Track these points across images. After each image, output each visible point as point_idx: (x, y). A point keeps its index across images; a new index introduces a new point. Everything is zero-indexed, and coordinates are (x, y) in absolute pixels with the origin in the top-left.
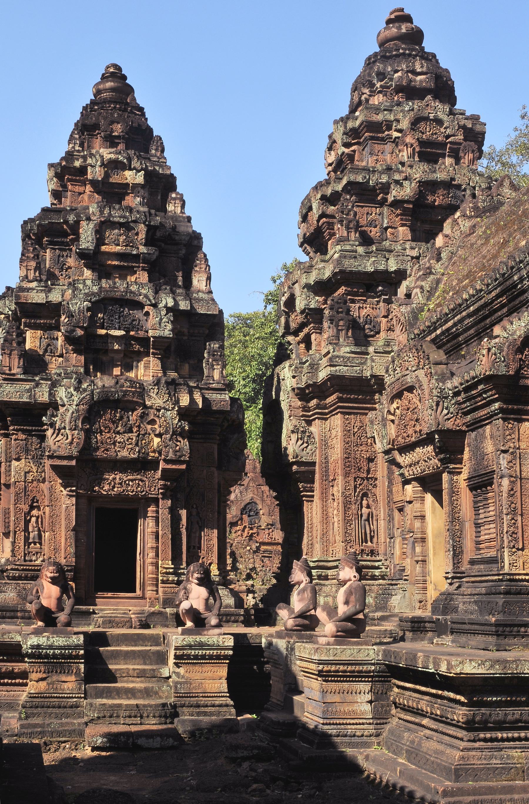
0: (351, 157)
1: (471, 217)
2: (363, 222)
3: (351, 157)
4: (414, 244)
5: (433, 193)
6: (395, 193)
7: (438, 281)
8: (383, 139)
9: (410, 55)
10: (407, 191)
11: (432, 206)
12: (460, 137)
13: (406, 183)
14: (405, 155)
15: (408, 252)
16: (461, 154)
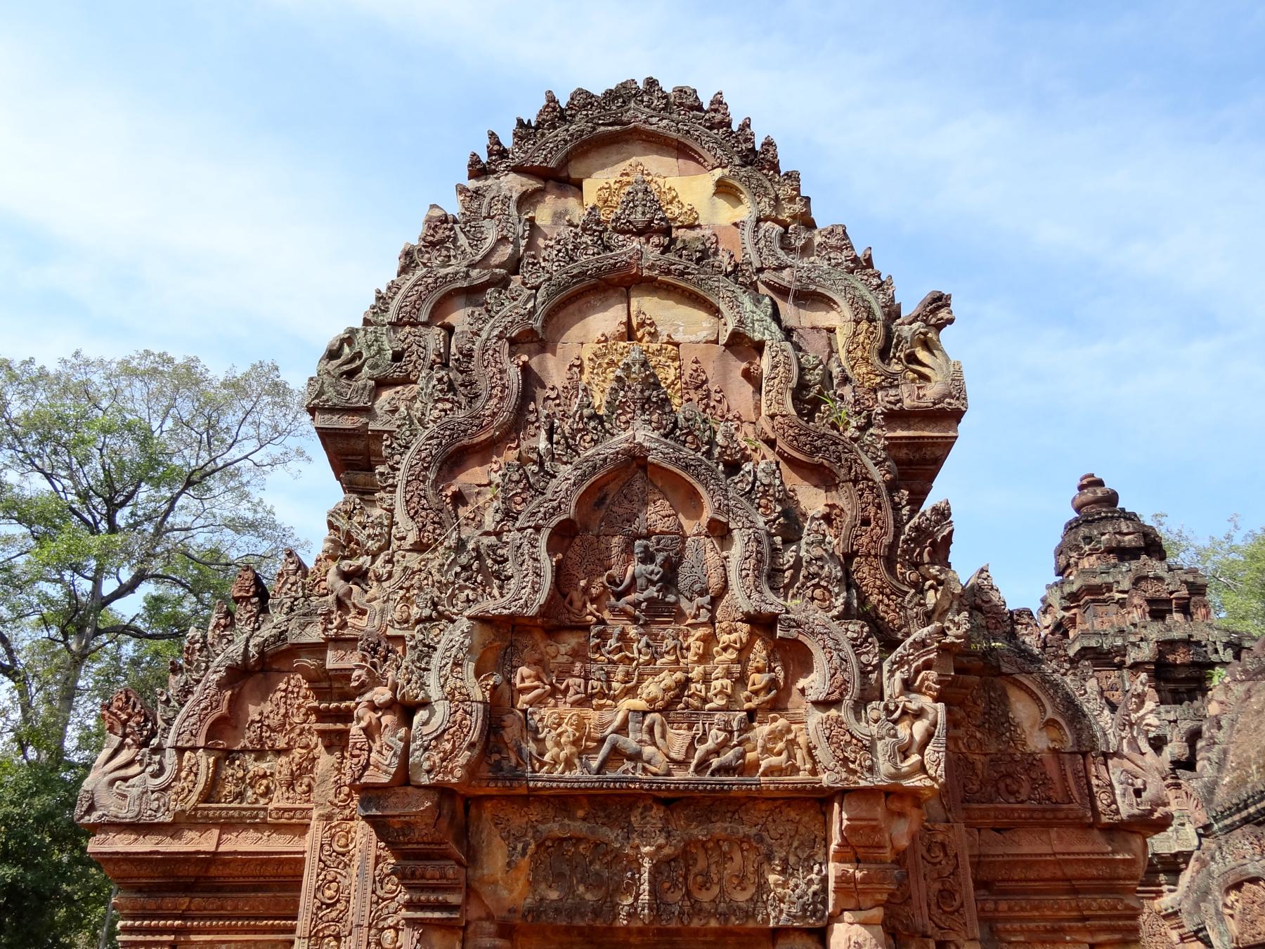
0: (1073, 621)
1: (1242, 681)
2: (1105, 687)
3: (1073, 621)
4: (1168, 707)
5: (1173, 652)
6: (1133, 656)
7: (1225, 752)
8: (1104, 601)
9: (1112, 517)
10: (1146, 652)
11: (1175, 665)
12: (1184, 592)
13: (1143, 644)
14: (1136, 615)
15: (1164, 716)
16: (1192, 609)
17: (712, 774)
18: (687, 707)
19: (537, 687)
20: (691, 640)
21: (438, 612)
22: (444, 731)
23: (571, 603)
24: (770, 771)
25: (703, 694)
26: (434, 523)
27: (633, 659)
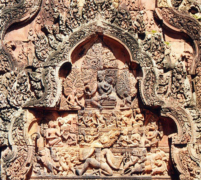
17: (131, 174)
18: (121, 146)
19: (55, 138)
20: (123, 116)
21: (10, 105)
22: (16, 159)
23: (69, 100)
24: (156, 173)
25: (128, 141)
26: (4, 61)
27: (97, 126)
